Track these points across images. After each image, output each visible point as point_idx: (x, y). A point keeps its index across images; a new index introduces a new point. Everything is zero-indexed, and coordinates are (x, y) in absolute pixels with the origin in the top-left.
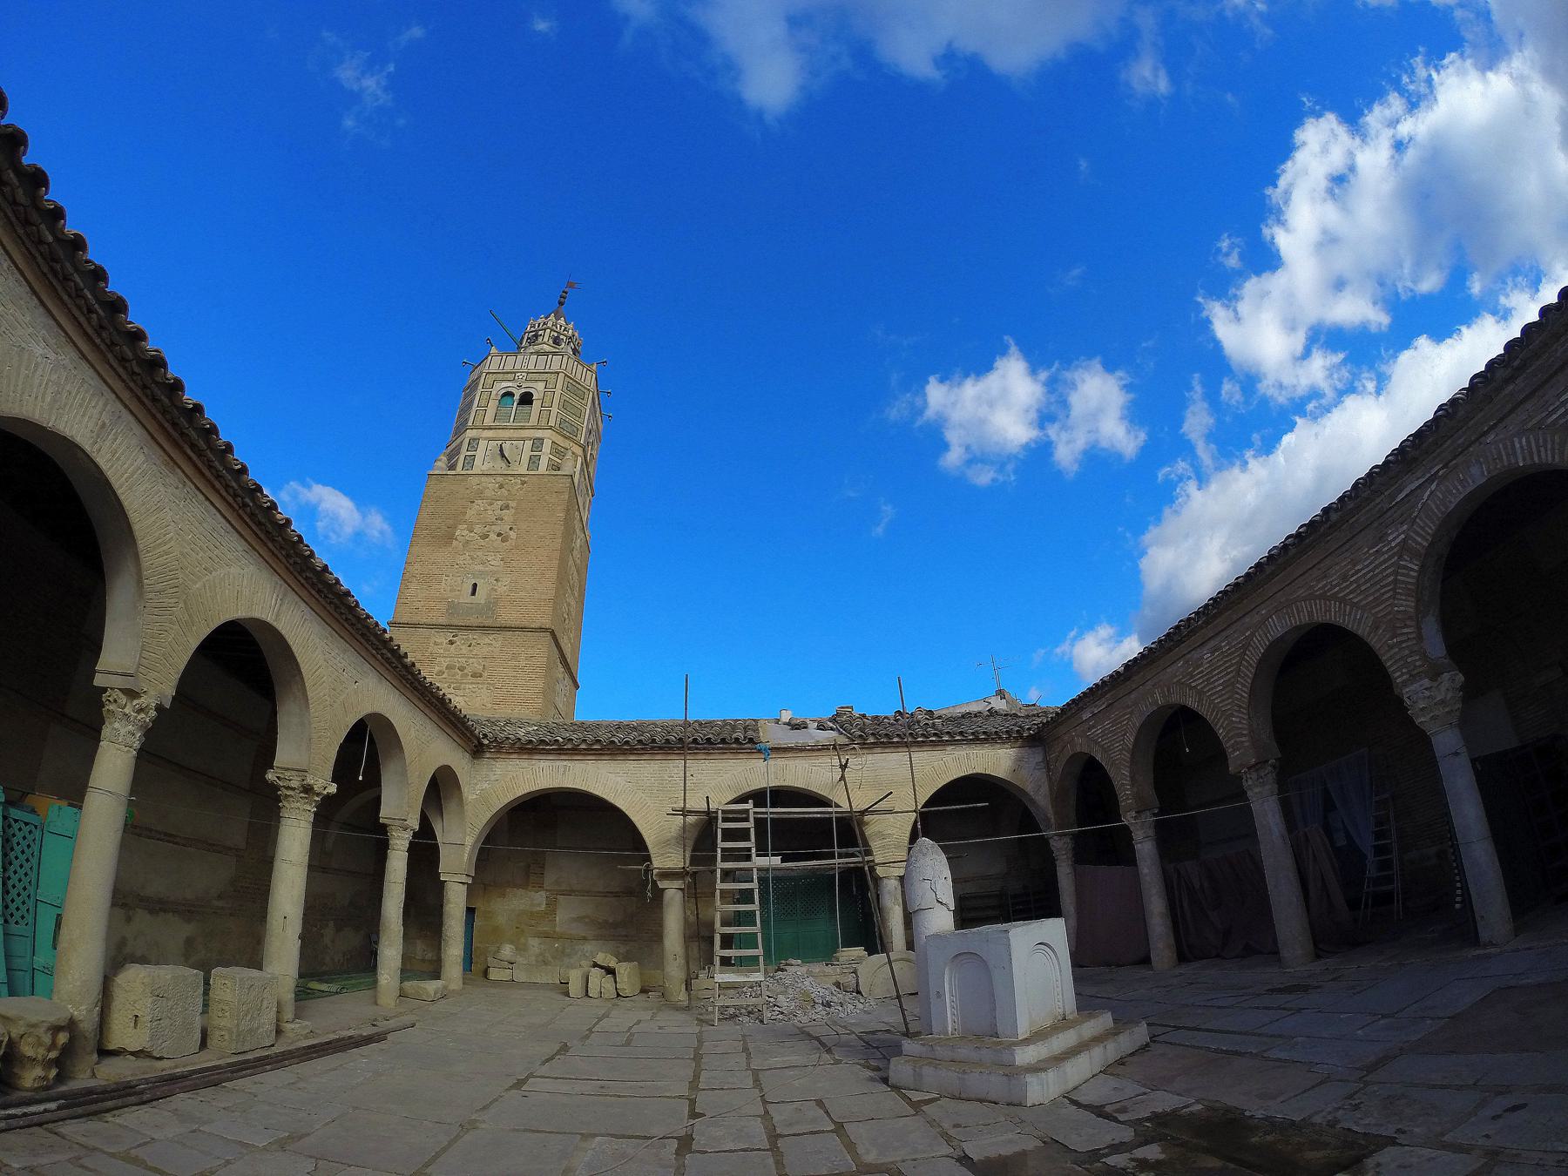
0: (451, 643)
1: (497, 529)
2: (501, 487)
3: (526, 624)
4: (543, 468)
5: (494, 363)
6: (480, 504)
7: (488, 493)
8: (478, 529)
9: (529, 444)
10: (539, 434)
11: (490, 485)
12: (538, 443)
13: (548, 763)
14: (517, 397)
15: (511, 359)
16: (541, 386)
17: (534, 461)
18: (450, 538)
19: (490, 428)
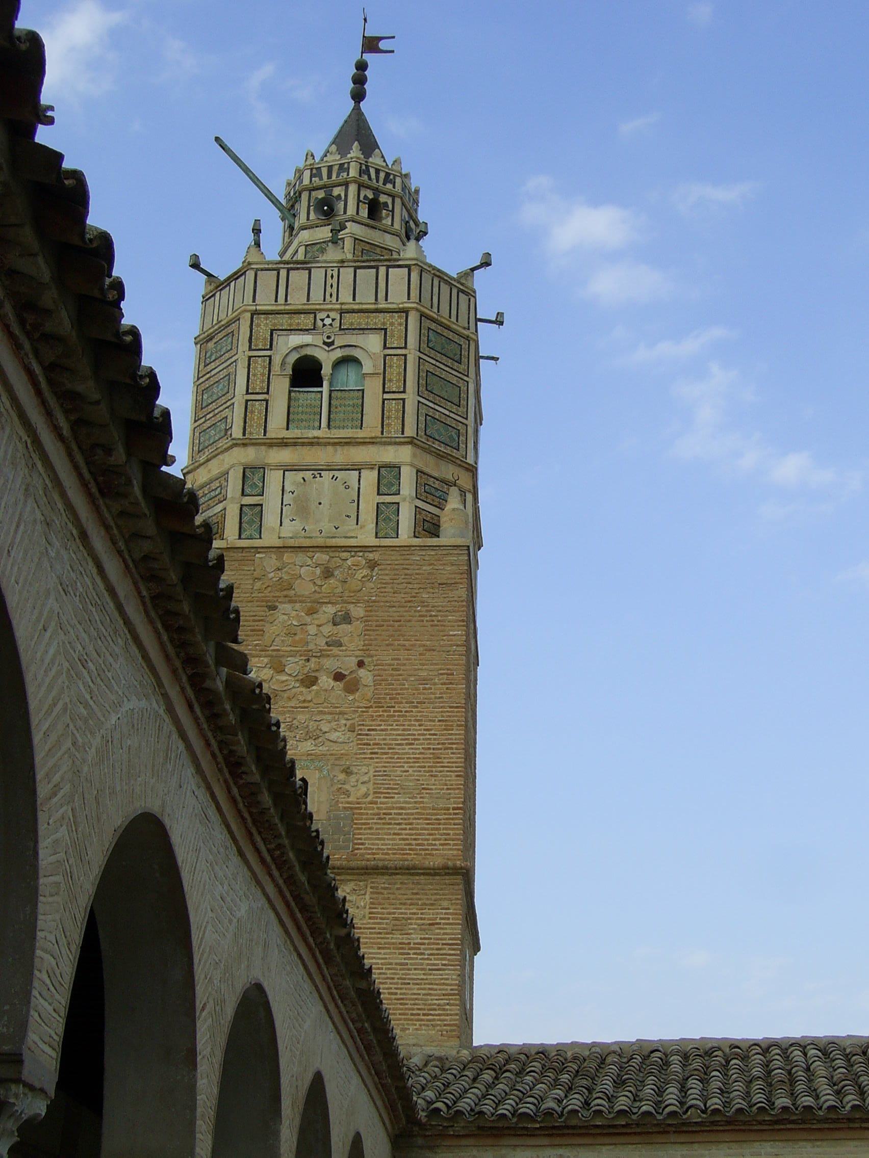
2: (328, 573)
3: (413, 859)
6: (287, 614)
7: (304, 588)
8: (293, 665)
9: (370, 477)
10: (389, 455)
11: (305, 569)
15: (298, 278)
16: (373, 342)
17: (385, 516)
19: (283, 443)
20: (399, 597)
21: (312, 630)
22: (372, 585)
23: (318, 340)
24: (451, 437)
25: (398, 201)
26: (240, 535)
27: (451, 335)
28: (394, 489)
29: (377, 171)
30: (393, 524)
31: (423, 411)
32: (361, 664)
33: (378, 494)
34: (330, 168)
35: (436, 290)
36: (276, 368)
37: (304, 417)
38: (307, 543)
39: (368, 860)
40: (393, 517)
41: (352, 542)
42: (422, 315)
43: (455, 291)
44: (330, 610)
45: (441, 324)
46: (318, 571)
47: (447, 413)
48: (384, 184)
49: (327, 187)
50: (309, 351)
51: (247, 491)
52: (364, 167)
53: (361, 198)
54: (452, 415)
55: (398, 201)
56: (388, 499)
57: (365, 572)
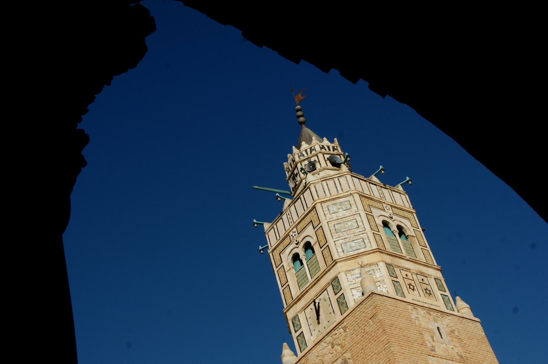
5: (272, 239)
9: (330, 289)
12: (335, 283)
16: (310, 230)
20: (359, 337)
22: (349, 338)
23: (293, 245)
25: (320, 156)
28: (339, 288)
29: (306, 151)
30: (345, 304)
33: (336, 295)
34: (291, 164)
35: (325, 187)
36: (286, 268)
37: (302, 282)
40: (344, 301)
42: (321, 202)
43: (336, 180)
45: (334, 199)
46: (330, 347)
48: (311, 153)
50: (293, 252)
51: (296, 329)
52: (300, 154)
55: (320, 156)
57: (343, 334)
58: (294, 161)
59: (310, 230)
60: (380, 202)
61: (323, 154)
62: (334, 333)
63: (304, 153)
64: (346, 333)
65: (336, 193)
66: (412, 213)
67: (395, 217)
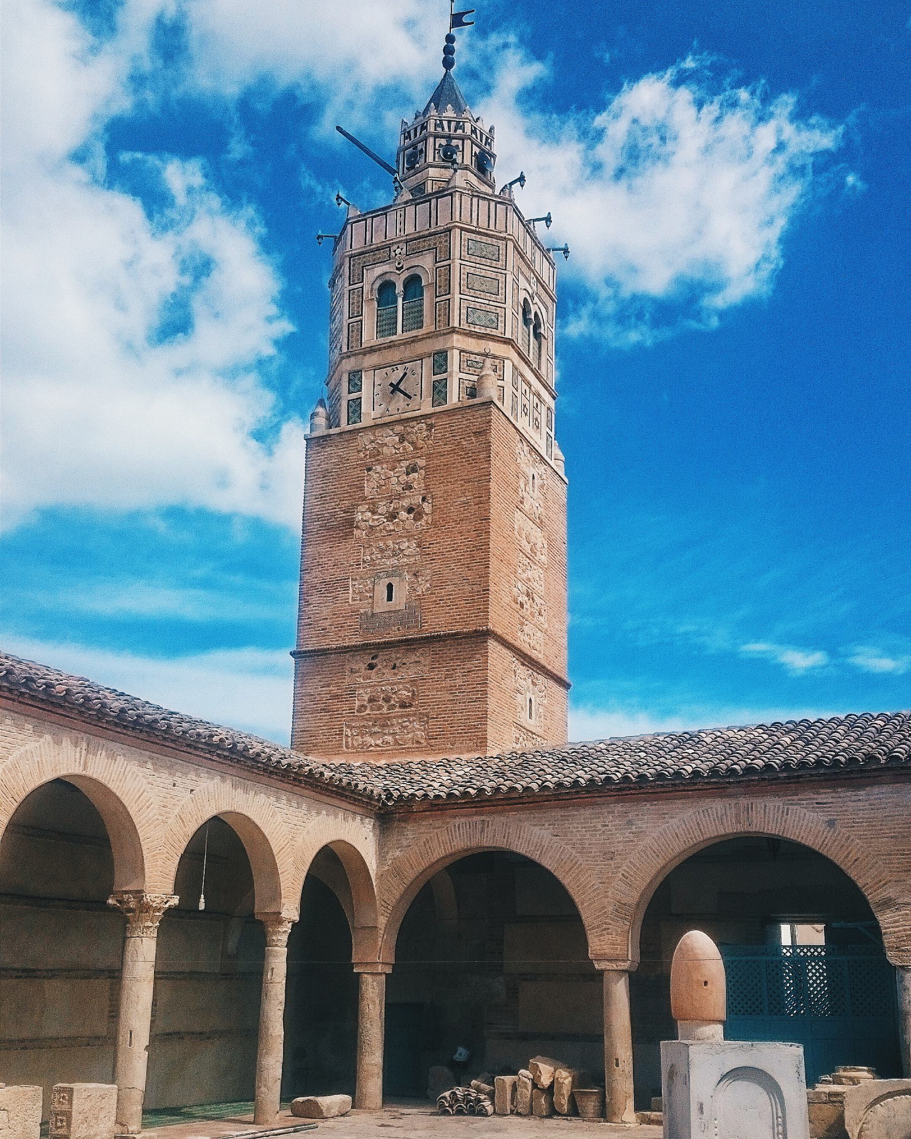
0: (371, 667)
1: (406, 503)
2: (402, 439)
4: (454, 397)
9: (428, 362)
11: (390, 438)
12: (440, 360)
13: (463, 820)
14: (399, 288)
18: (350, 524)
19: (372, 350)
20: (448, 448)
21: (394, 480)
24: (491, 321)
25: (468, 143)
26: (348, 421)
27: (489, 240)
29: (449, 122)
31: (464, 304)
32: (424, 499)
34: (416, 129)
38: (387, 419)
39: (431, 633)
41: (417, 413)
44: (405, 464)
46: (397, 439)
47: (487, 302)
48: (455, 131)
49: (414, 146)
50: (387, 277)
52: (438, 122)
53: (437, 147)
54: (491, 303)
55: (468, 143)
56: (438, 377)
57: (425, 433)
58: (424, 127)
59: (426, 262)
60: (529, 268)
61: (472, 143)
62: (411, 424)
63: (445, 124)
64: (428, 433)
65: (486, 226)
66: (553, 301)
67: (536, 299)
